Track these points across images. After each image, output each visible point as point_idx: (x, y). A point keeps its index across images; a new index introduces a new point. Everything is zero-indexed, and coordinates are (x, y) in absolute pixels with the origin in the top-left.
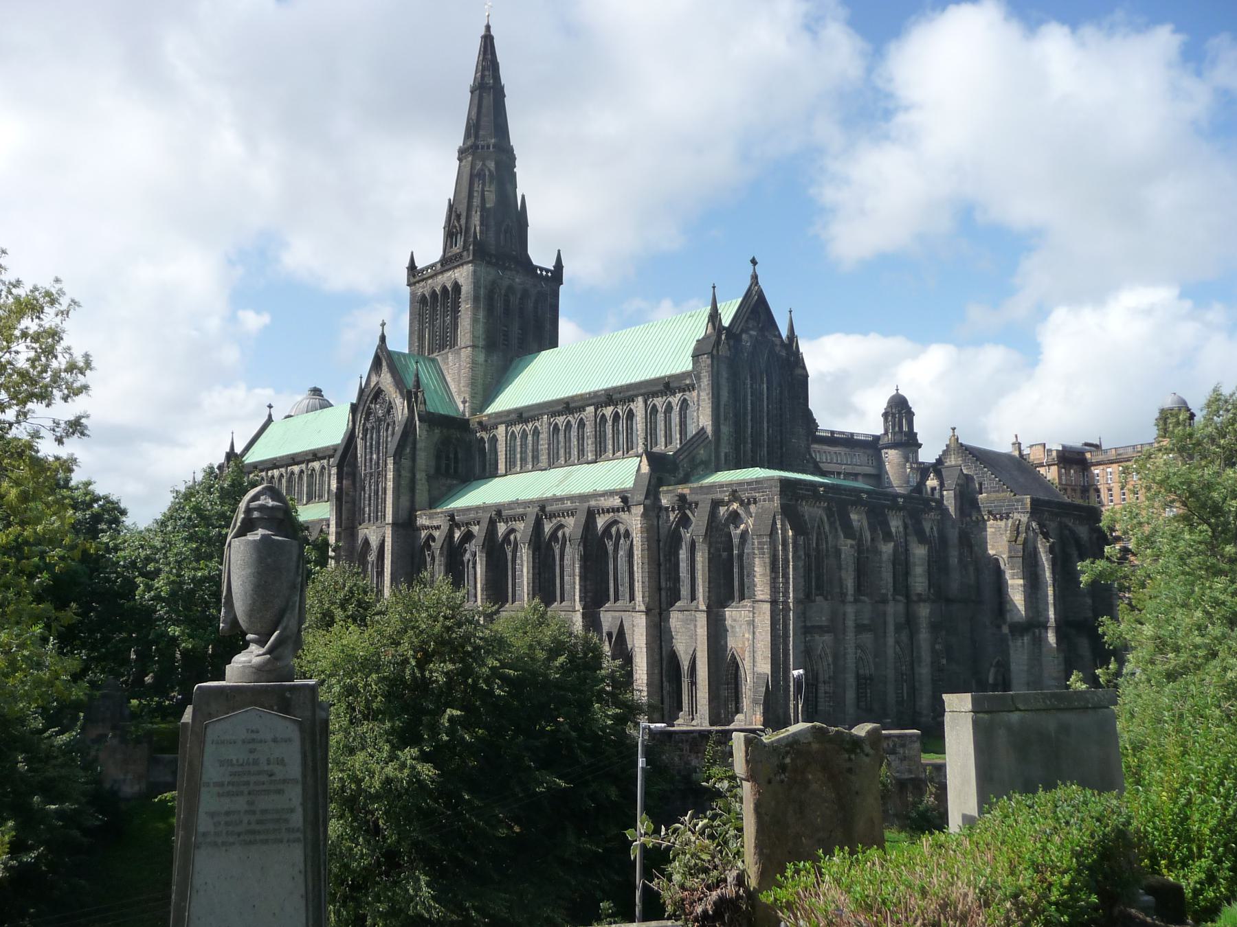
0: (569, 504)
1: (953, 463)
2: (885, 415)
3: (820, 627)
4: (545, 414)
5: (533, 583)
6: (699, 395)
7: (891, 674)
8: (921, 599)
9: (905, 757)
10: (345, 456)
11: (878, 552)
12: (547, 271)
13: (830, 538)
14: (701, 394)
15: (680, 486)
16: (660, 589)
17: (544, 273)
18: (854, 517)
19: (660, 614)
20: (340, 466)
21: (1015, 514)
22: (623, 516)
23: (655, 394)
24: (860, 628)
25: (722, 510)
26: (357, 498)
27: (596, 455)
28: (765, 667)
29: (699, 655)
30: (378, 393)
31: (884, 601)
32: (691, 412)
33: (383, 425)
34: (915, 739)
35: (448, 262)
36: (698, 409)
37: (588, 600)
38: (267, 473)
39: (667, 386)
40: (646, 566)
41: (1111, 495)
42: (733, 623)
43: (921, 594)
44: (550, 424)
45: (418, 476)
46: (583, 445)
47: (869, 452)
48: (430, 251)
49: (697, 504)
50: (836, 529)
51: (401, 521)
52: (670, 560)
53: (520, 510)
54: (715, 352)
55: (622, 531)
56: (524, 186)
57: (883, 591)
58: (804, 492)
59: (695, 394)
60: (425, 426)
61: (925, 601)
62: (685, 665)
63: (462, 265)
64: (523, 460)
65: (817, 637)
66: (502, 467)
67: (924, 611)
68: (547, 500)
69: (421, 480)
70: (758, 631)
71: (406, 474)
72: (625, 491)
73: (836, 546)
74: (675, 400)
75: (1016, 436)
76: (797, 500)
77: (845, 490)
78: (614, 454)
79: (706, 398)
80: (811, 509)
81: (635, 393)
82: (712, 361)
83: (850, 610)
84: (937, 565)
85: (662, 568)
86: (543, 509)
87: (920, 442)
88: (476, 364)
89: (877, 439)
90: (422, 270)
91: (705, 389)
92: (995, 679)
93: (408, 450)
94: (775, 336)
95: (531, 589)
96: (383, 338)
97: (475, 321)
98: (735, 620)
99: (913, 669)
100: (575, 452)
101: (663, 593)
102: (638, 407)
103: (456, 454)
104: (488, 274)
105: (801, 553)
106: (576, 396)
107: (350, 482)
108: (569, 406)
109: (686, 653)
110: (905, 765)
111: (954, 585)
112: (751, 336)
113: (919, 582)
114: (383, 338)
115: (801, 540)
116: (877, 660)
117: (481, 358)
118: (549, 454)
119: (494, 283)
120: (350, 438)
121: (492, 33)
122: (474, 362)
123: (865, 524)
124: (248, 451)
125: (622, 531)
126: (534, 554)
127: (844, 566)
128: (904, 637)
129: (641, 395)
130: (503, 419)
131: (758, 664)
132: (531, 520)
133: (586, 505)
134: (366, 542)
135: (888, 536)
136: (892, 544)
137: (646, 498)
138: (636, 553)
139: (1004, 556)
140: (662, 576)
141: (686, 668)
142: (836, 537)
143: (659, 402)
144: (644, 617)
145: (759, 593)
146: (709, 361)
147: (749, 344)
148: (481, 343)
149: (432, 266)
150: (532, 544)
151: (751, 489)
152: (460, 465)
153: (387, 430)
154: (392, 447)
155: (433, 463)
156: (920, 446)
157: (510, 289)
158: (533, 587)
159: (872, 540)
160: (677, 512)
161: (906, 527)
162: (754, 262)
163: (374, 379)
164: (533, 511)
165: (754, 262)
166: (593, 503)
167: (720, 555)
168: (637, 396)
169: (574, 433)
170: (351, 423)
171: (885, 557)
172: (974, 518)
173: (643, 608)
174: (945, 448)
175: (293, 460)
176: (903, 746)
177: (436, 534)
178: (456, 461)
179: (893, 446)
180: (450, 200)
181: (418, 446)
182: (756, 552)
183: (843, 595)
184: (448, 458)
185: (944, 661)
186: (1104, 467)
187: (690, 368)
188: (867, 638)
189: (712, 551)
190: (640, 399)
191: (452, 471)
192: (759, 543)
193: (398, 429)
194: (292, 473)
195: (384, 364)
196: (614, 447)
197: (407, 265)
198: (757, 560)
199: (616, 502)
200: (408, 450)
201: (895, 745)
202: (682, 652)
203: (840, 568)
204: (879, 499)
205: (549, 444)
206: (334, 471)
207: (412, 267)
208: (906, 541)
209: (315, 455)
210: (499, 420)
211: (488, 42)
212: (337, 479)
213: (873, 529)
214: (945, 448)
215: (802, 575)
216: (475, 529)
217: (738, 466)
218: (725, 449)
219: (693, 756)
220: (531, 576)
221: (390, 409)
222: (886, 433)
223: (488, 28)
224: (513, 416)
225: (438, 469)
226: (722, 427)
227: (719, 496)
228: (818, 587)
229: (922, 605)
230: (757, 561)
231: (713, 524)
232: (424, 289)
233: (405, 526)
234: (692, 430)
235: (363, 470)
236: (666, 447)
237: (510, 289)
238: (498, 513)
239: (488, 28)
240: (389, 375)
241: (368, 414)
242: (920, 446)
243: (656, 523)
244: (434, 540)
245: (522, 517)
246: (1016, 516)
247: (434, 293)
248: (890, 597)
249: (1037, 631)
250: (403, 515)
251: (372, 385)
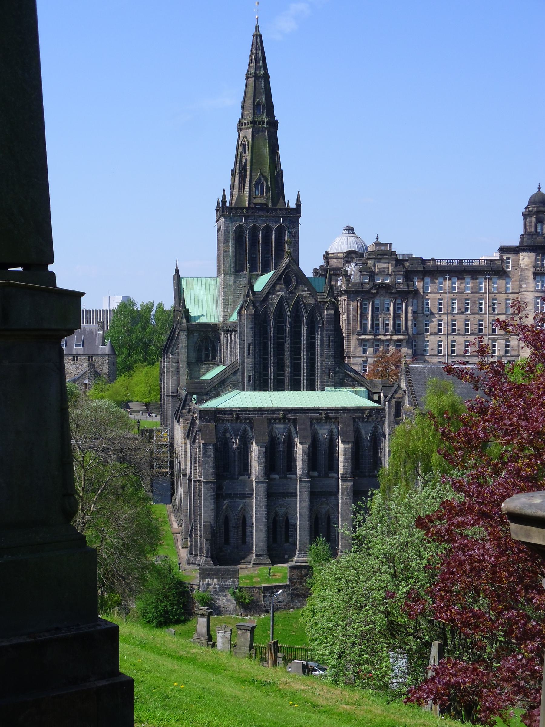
58: (223, 416)
65: (238, 500)
69: (183, 367)
114: (177, 271)
121: (261, 32)
122: (226, 286)
148: (231, 270)
184: (207, 349)
204: (307, 413)
211: (258, 39)
223: (257, 28)
239: (257, 28)
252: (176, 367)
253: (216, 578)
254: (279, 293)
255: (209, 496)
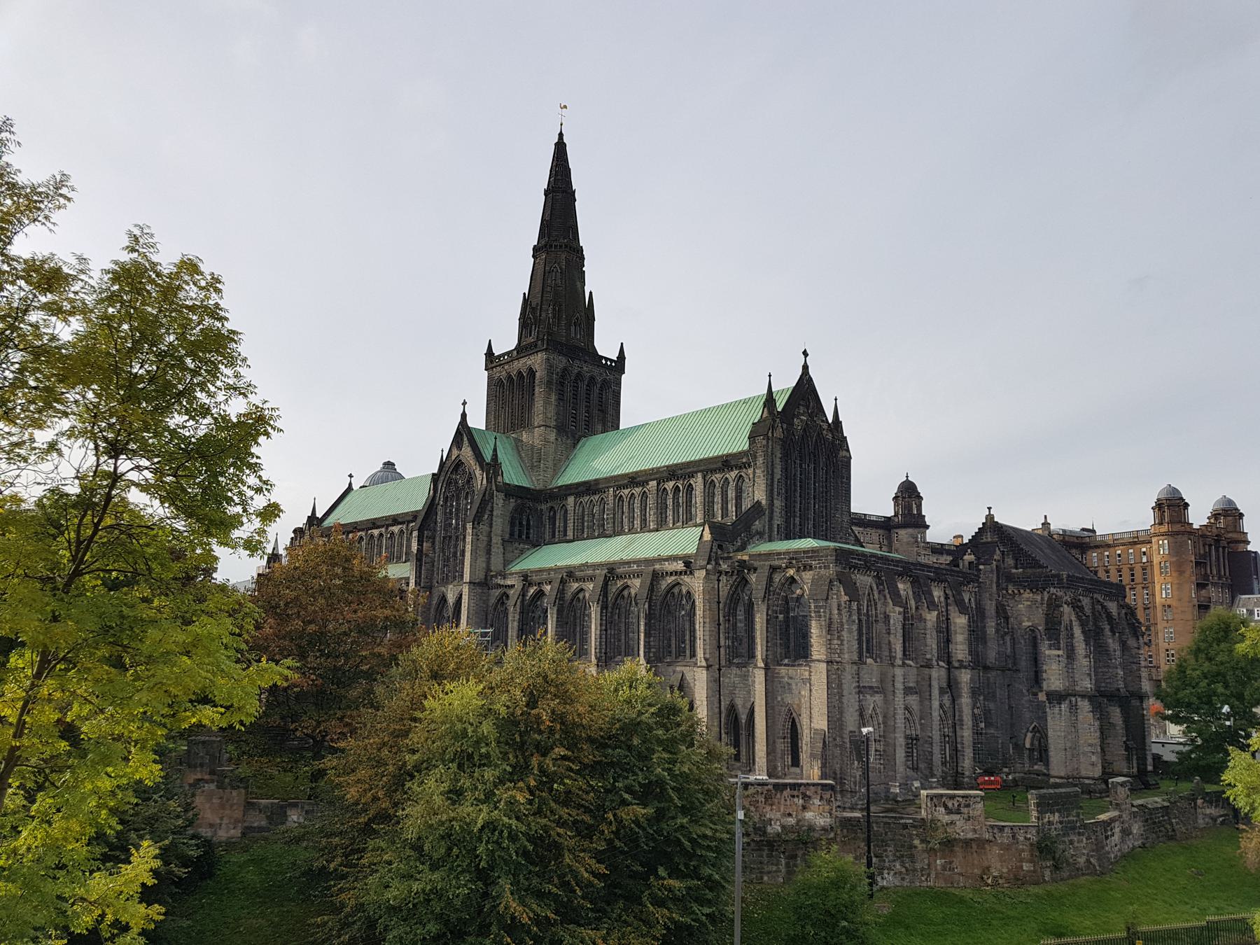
0: (635, 567)
1: (989, 540)
2: (896, 498)
3: (871, 688)
4: (611, 487)
5: (601, 638)
6: (754, 473)
7: (936, 736)
8: (962, 666)
9: (969, 817)
10: (425, 520)
11: (922, 619)
12: (612, 361)
13: (879, 606)
14: (757, 471)
15: (740, 553)
16: (719, 647)
17: (609, 363)
18: (901, 586)
19: (719, 670)
20: (421, 530)
21: (1052, 589)
22: (686, 579)
23: (713, 471)
24: (908, 691)
25: (777, 578)
26: (436, 559)
27: (658, 525)
28: (821, 723)
29: (756, 709)
30: (459, 464)
31: (928, 666)
32: (747, 485)
33: (463, 494)
34: (979, 799)
35: (522, 349)
36: (754, 485)
37: (652, 655)
38: (348, 535)
39: (726, 463)
40: (707, 625)
41: (1133, 575)
42: (790, 681)
43: (962, 661)
44: (615, 496)
45: (494, 541)
46: (645, 515)
47: (881, 532)
48: (507, 341)
49: (755, 569)
50: (885, 596)
51: (477, 581)
52: (729, 620)
53: (590, 572)
54: (770, 434)
55: (684, 591)
56: (592, 283)
57: (928, 656)
59: (750, 471)
60: (501, 495)
61: (965, 668)
62: (743, 718)
63: (537, 352)
64: (591, 528)
65: (868, 697)
66: (570, 534)
67: (965, 677)
68: (614, 563)
69: (497, 544)
70: (814, 688)
71: (483, 538)
72: (689, 556)
73: (885, 613)
74: (734, 474)
75: (1046, 517)
76: (850, 569)
77: (892, 561)
78: (674, 524)
79: (762, 475)
80: (862, 578)
81: (695, 469)
82: (768, 443)
83: (899, 672)
84: (976, 635)
85: (721, 627)
86: (612, 571)
87: (928, 524)
88: (548, 442)
89: (889, 518)
90: (500, 356)
91: (760, 468)
92: (1032, 744)
93: (486, 516)
94: (823, 421)
95: (598, 643)
96: (464, 415)
97: (547, 403)
98: (791, 678)
99: (955, 732)
100: (637, 523)
101: (721, 649)
102: (698, 482)
103: (528, 521)
104: (561, 362)
105: (855, 617)
106: (641, 471)
107: (429, 544)
108: (634, 480)
109: (744, 706)
110: (968, 826)
111: (992, 655)
112: (802, 421)
113: (960, 650)
114: (464, 415)
115: (854, 606)
116: (923, 721)
117: (552, 437)
118: (614, 523)
119: (565, 369)
120: (431, 506)
123: (911, 593)
124: (329, 515)
125: (684, 591)
126: (602, 612)
127: (892, 632)
128: (947, 701)
129: (700, 471)
130: (572, 491)
131: (814, 720)
132: (600, 580)
133: (651, 568)
134: (443, 599)
135: (932, 605)
136: (936, 612)
137: (708, 564)
138: (698, 612)
139: (1040, 628)
140: (721, 635)
141: (744, 721)
142: (885, 604)
143: (717, 477)
144: (705, 672)
145: (816, 653)
146: (764, 442)
147: (800, 428)
149: (508, 353)
150: (600, 602)
151: (807, 557)
152: (532, 531)
153: (466, 498)
154: (471, 514)
155: (508, 530)
156: (928, 527)
157: (579, 375)
158: (600, 642)
159: (917, 608)
160: (734, 577)
161: (947, 598)
162: (805, 354)
163: (455, 452)
164: (601, 573)
165: (805, 354)
166: (657, 567)
167: (777, 617)
168: (696, 472)
169: (637, 505)
170: (432, 492)
171: (929, 625)
172: (1010, 592)
173: (704, 664)
174: (981, 526)
175: (374, 523)
176: (968, 806)
177: (511, 592)
178: (528, 524)
179: (904, 526)
180: (525, 294)
181: (495, 513)
182: (813, 615)
183: (892, 658)
184: (521, 523)
185: (982, 725)
186: (1102, 550)
187: (744, 445)
188: (913, 700)
189: (770, 612)
190: (700, 475)
191: (524, 537)
192: (816, 607)
193: (477, 499)
194: (372, 536)
195: (465, 439)
196: (674, 518)
197: (485, 352)
198: (813, 622)
199: (680, 566)
200: (486, 516)
201: (959, 805)
202: (740, 706)
203: (889, 633)
205: (614, 515)
206: (415, 534)
207: (490, 353)
208: (947, 610)
209: (395, 520)
210: (568, 492)
212: (418, 541)
213: (917, 597)
214: (981, 526)
215: (856, 638)
216: (547, 588)
217: (788, 536)
218: (777, 521)
219: (768, 808)
220: (598, 632)
221: (471, 478)
222: (896, 515)
224: (581, 488)
225: (512, 534)
226: (775, 501)
227: (776, 563)
228: (868, 651)
229: (963, 670)
230: (814, 623)
231: (771, 588)
232: (501, 373)
233: (482, 584)
234: (746, 504)
235: (440, 534)
236: (722, 519)
237: (579, 375)
238: (570, 574)
240: (469, 449)
241: (449, 484)
242: (928, 527)
243: (716, 586)
244: (508, 597)
245: (591, 579)
246: (1053, 590)
247: (510, 377)
248: (934, 663)
249: (1073, 699)
250: (482, 576)
251: (453, 458)
252: (485, 543)
253: (1059, 811)
254: (802, 417)
255: (855, 688)
